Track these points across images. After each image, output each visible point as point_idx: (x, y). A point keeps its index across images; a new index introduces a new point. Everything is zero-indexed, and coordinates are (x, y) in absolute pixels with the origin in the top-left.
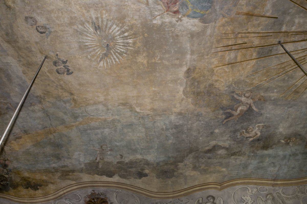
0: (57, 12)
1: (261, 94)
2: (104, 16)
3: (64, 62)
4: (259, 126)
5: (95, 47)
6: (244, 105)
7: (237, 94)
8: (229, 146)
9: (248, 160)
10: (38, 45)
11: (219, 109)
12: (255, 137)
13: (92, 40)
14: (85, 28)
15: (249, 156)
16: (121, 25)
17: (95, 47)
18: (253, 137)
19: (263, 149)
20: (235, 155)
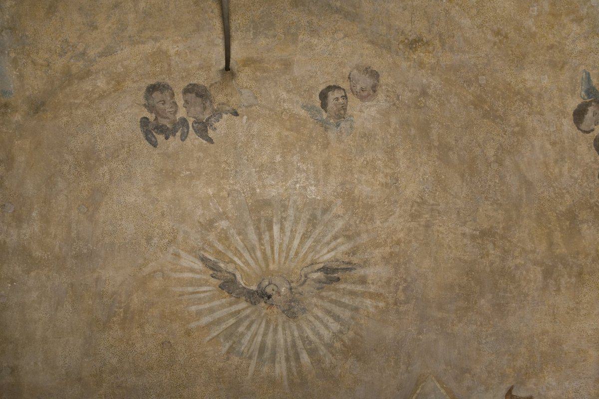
0: (388, 171)
2: (368, 302)
3: (203, 129)
5: (264, 253)
10: (277, 66)
13: (289, 249)
14: (335, 238)
16: (338, 345)
17: (264, 253)
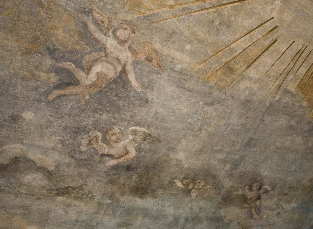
1: (155, 46)
4: (135, 133)
6: (108, 62)
7: (96, 22)
8: (56, 167)
9: (97, 214)
11: (43, 51)
12: (121, 160)
15: (100, 205)
18: (118, 158)
19: (136, 194)
20: (66, 195)
